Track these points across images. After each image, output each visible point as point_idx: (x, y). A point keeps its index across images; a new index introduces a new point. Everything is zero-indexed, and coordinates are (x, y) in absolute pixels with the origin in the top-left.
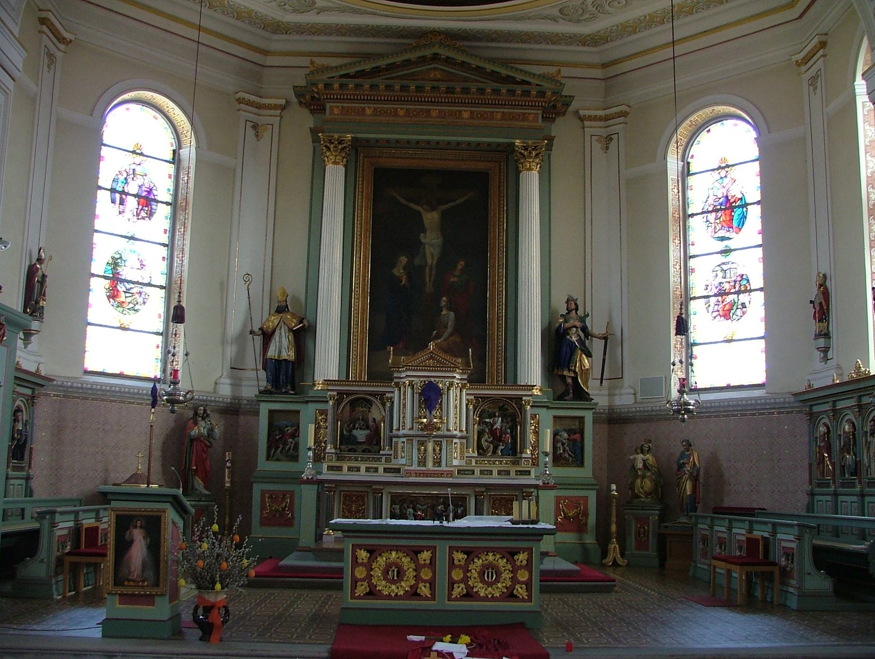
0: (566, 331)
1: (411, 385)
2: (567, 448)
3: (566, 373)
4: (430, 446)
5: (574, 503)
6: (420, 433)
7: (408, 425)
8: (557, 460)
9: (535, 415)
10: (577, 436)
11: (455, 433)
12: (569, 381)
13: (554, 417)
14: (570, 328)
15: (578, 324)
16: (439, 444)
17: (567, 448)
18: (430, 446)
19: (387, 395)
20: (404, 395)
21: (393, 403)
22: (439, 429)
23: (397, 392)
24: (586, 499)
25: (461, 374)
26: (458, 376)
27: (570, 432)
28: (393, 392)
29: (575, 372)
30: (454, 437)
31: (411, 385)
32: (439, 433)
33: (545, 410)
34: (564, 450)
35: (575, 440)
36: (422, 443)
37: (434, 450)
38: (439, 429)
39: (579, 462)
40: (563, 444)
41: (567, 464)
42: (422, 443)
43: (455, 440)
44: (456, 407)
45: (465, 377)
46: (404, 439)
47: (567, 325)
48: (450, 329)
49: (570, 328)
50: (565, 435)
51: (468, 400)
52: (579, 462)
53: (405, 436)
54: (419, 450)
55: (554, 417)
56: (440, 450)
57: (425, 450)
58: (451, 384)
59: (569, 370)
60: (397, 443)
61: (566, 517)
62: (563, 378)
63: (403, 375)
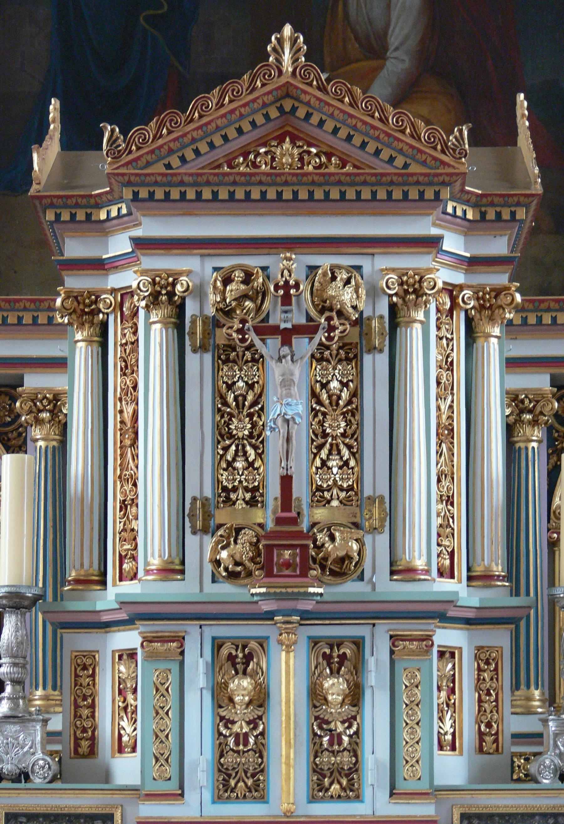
1: (165, 295)
4: (287, 669)
6: (227, 590)
7: (154, 547)
11: (446, 586)
16: (340, 658)
18: (287, 669)
19: (34, 381)
20: (128, 368)
21: (64, 430)
22: (342, 568)
23: (82, 355)
25: (469, 228)
26: (453, 243)
28: (60, 364)
30: (441, 612)
31: (165, 295)
32: (350, 588)
36: (237, 659)
37: (316, 696)
38: (342, 568)
42: (237, 659)
43: (446, 636)
44: (446, 433)
45: (499, 246)
46: (129, 639)
48: (398, 64)
51: (513, 398)
53: (136, 614)
54: (221, 697)
56: (355, 696)
57: (261, 699)
58: (413, 289)
60: (86, 665)
63: (119, 245)
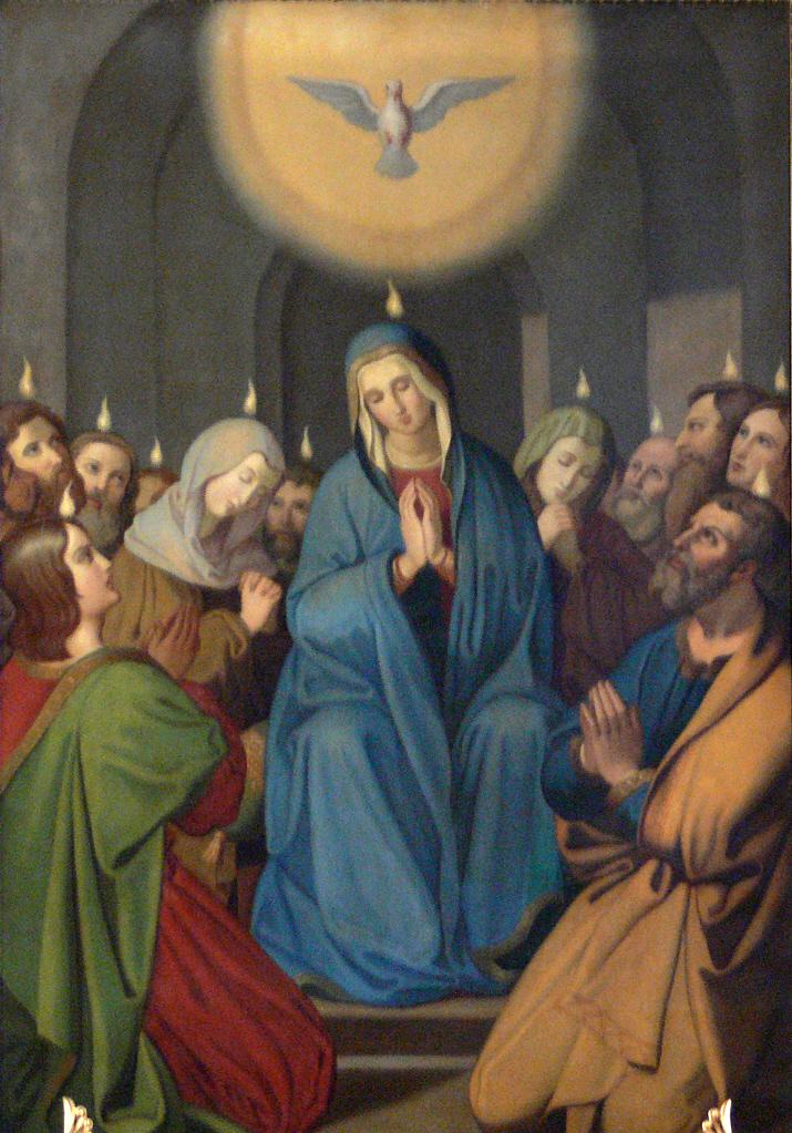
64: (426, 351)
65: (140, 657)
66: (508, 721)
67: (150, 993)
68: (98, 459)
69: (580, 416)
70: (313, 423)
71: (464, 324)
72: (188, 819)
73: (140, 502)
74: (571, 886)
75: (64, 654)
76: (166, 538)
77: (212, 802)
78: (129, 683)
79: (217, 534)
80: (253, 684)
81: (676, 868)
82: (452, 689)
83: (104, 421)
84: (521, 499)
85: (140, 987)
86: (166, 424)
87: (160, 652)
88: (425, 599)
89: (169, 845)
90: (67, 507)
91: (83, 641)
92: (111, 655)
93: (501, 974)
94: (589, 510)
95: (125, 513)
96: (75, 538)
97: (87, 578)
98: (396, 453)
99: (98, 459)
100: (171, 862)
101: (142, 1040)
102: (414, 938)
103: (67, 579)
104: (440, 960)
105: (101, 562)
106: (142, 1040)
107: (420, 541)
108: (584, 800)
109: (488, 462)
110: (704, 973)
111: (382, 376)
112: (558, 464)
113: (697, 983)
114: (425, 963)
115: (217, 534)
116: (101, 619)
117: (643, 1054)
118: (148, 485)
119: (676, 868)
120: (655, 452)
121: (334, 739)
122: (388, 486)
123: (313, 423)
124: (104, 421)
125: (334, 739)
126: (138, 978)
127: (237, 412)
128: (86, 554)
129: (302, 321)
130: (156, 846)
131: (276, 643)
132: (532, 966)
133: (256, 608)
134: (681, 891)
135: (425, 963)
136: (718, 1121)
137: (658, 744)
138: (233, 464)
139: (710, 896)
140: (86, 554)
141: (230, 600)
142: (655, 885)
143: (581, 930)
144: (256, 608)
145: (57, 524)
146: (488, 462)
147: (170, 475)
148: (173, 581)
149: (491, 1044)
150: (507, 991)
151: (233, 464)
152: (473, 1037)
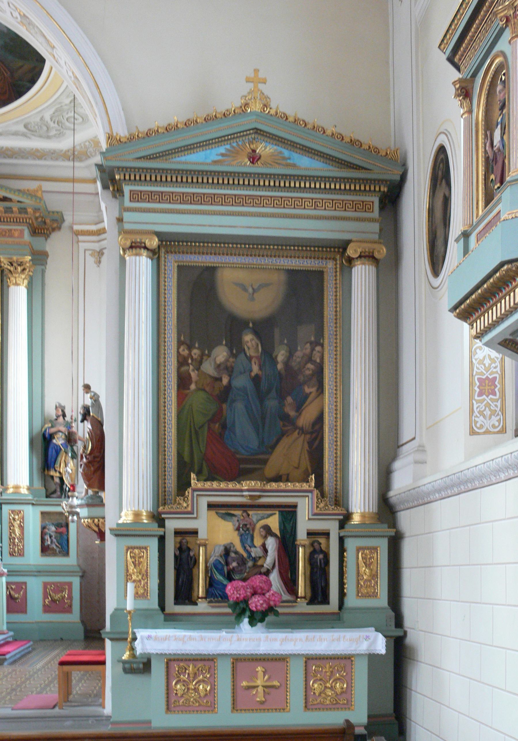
0: (52, 436)
2: (55, 540)
3: (52, 473)
5: (59, 587)
8: (45, 550)
9: (20, 512)
10: (63, 529)
12: (57, 480)
13: (43, 513)
14: (56, 433)
15: (63, 429)
17: (55, 540)
24: (70, 584)
27: (58, 526)
29: (60, 473)
33: (30, 507)
34: (52, 542)
35: (61, 533)
39: (67, 553)
40: (51, 537)
41: (54, 554)
47: (53, 430)
49: (56, 433)
50: (53, 528)
52: (67, 553)
55: (43, 513)
59: (56, 471)
61: (53, 601)
62: (52, 477)
64: (256, 333)
65: (204, 390)
66: (272, 403)
67: (205, 454)
68: (196, 352)
69: (286, 347)
70: (236, 346)
71: (263, 328)
72: (212, 420)
73: (204, 360)
74: (283, 434)
75: (189, 389)
76: (208, 367)
77: (217, 417)
78: (201, 394)
79: (218, 367)
80: (225, 395)
81: (302, 431)
82: (261, 397)
83: (197, 345)
84: (274, 361)
85: (203, 452)
86: (208, 346)
87: (207, 389)
88: (256, 380)
89: (209, 425)
90: (190, 361)
91: (193, 387)
92: (198, 389)
93: (270, 450)
94: (287, 364)
95: (201, 363)
96: (191, 367)
97: (194, 375)
98: (251, 352)
99: (196, 352)
100: (209, 428)
101: (204, 462)
102: (254, 443)
103: (190, 375)
104: (259, 447)
105: (196, 372)
106: (204, 462)
107: (255, 369)
108: (285, 418)
109: (268, 355)
110: (307, 450)
111: (248, 338)
112: (281, 356)
113: (306, 452)
114: (256, 448)
115: (218, 367)
116: (196, 383)
117: (296, 465)
118: (205, 358)
119: (302, 431)
120: (299, 354)
121: (240, 406)
122: (250, 359)
123: (236, 346)
124: (197, 345)
125: (240, 406)
126: (203, 449)
127: (221, 344)
128: (193, 370)
129: (233, 328)
130: (206, 425)
131: (228, 388)
132: (276, 449)
133: (225, 381)
134: (303, 435)
135: (256, 448)
136: (312, 478)
137: (299, 408)
138: (221, 354)
139: (308, 436)
140: (193, 370)
141: (220, 379)
142: (298, 434)
143: (285, 442)
144: (225, 381)
145: (188, 365)
146: (268, 355)
147: (209, 356)
148: (210, 376)
149: (268, 463)
150: (271, 453)
151: (221, 354)
152: (265, 462)
